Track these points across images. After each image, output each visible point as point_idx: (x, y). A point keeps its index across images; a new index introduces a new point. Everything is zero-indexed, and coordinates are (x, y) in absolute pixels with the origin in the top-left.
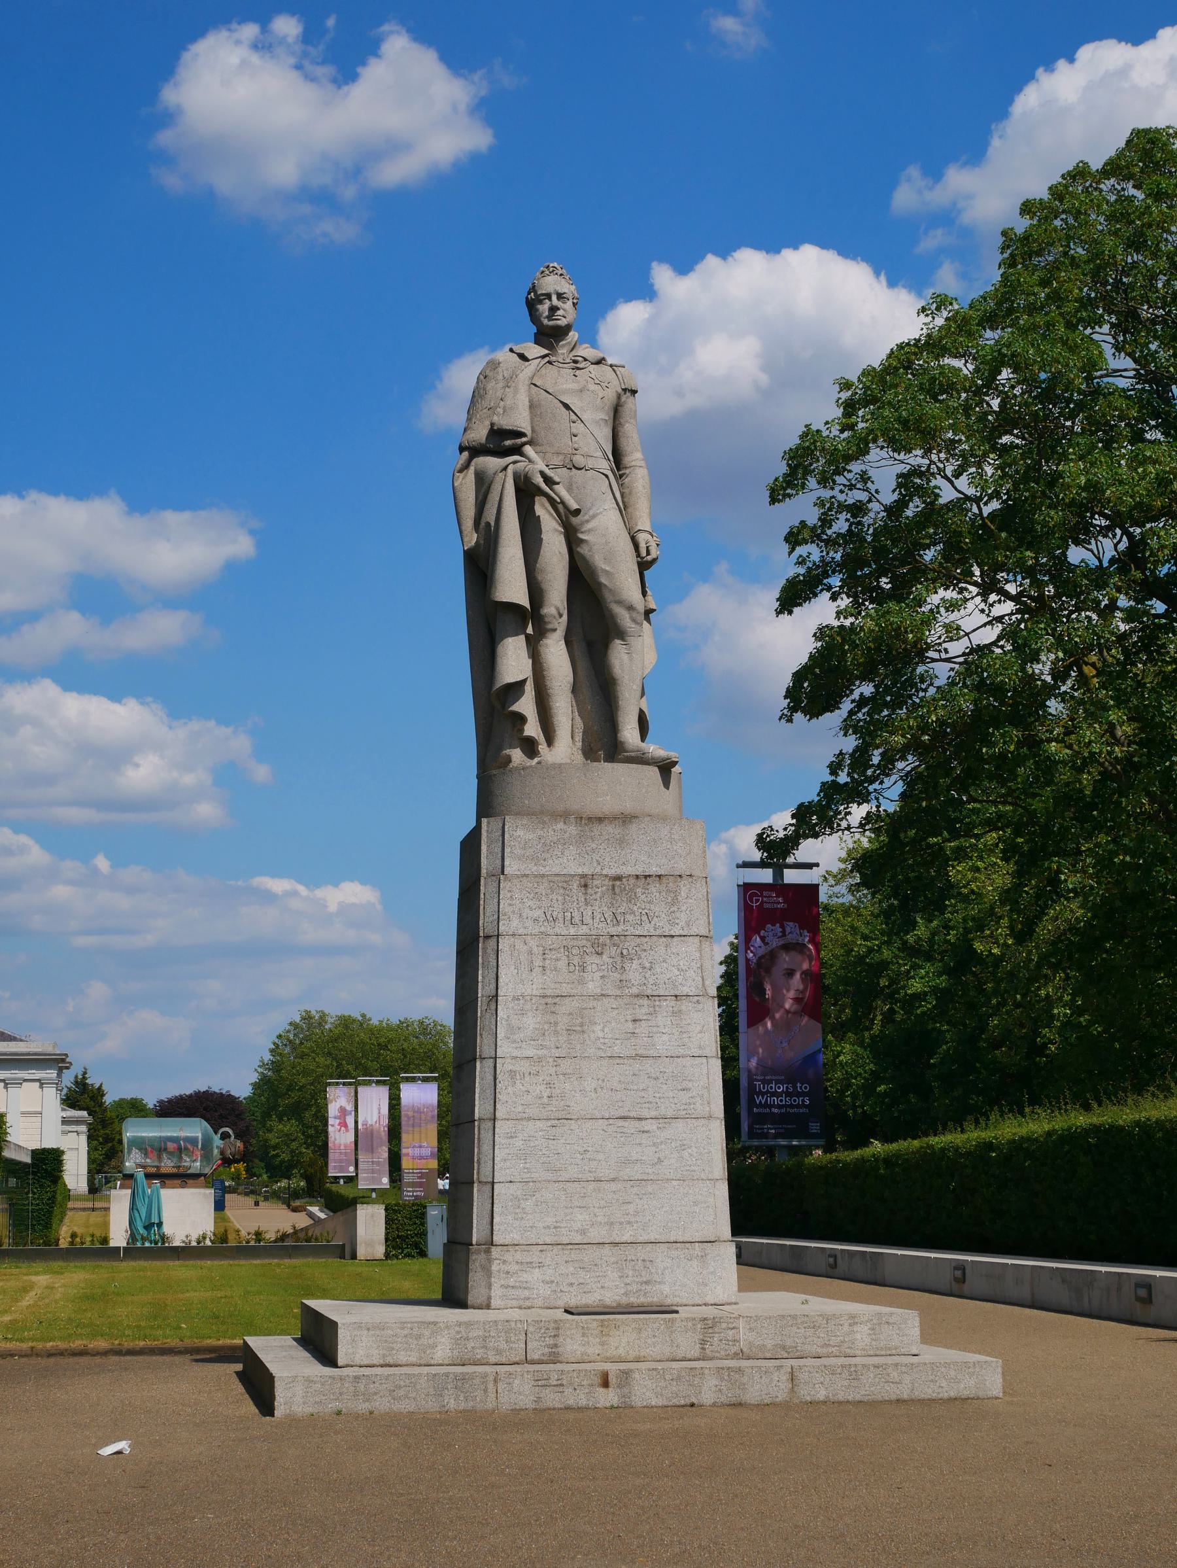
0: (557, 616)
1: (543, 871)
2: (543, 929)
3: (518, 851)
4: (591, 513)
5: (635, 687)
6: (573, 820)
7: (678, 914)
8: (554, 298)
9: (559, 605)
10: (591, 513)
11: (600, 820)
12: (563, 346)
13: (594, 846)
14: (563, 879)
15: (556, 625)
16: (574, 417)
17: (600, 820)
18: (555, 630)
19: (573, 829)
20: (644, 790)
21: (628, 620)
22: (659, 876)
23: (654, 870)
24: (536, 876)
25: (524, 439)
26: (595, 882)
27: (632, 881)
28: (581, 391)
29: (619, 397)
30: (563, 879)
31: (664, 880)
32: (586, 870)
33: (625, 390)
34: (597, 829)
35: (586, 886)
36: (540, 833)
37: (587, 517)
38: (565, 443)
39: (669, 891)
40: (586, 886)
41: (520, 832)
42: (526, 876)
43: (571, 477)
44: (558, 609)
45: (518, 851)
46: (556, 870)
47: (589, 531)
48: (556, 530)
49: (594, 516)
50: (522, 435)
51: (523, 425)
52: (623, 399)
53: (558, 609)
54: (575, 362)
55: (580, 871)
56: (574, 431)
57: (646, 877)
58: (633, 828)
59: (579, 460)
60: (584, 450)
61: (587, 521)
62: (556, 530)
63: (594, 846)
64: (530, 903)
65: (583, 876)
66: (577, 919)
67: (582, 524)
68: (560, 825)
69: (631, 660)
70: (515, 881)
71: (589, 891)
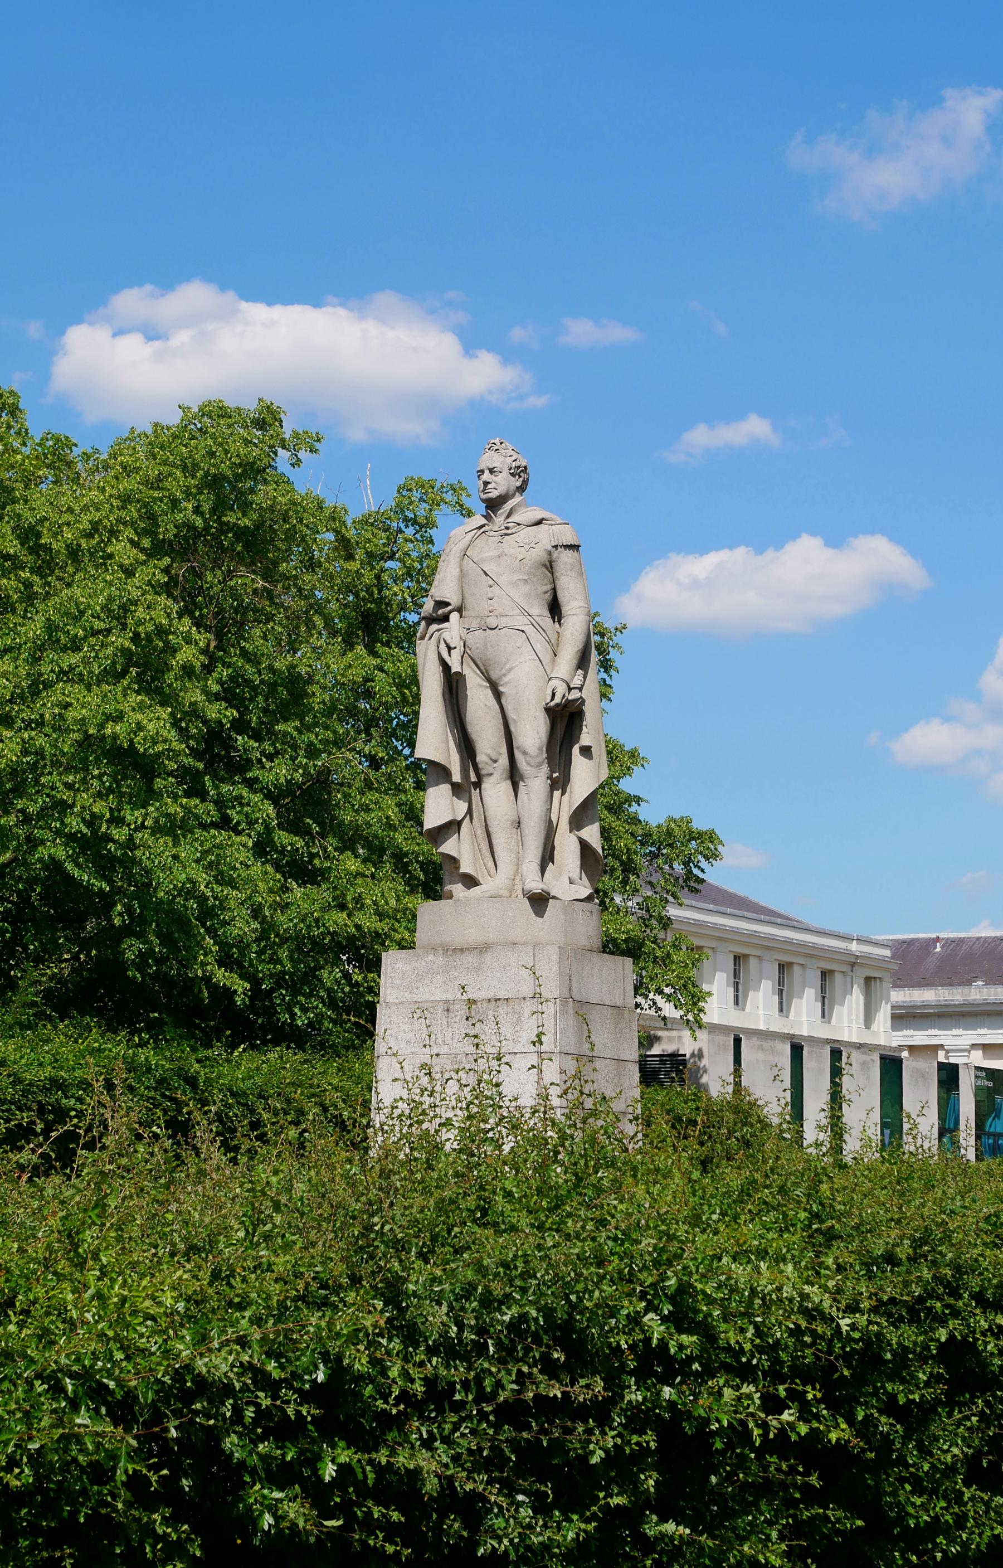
0: (490, 762)
1: (415, 998)
2: (413, 1050)
3: (398, 982)
4: (507, 667)
5: (532, 824)
6: (441, 952)
7: (520, 1033)
8: (487, 472)
9: (489, 751)
10: (507, 667)
11: (462, 950)
12: (502, 514)
13: (456, 974)
14: (431, 1004)
15: (491, 770)
16: (491, 582)
17: (462, 950)
18: (491, 774)
19: (440, 960)
20: (509, 921)
21: (524, 763)
22: (507, 999)
23: (503, 994)
24: (410, 1003)
25: (450, 608)
26: (456, 1007)
27: (485, 1004)
28: (499, 556)
29: (550, 554)
30: (431, 1004)
31: (511, 1002)
32: (449, 996)
33: (556, 547)
34: (460, 958)
35: (448, 1010)
36: (414, 964)
37: (504, 671)
38: (485, 606)
39: (514, 1013)
40: (448, 1010)
41: (399, 965)
42: (402, 1003)
43: (486, 638)
44: (489, 756)
45: (398, 982)
46: (425, 997)
47: (506, 683)
48: (481, 686)
49: (510, 670)
50: (448, 604)
51: (448, 595)
52: (555, 555)
53: (489, 756)
54: (507, 528)
55: (444, 998)
56: (490, 595)
57: (496, 1000)
58: (488, 956)
59: (492, 621)
60: (499, 611)
61: (505, 675)
62: (481, 686)
63: (456, 974)
64: (405, 1027)
65: (447, 1002)
66: (440, 1041)
67: (500, 678)
68: (431, 957)
69: (529, 799)
70: (394, 1008)
71: (451, 1015)
